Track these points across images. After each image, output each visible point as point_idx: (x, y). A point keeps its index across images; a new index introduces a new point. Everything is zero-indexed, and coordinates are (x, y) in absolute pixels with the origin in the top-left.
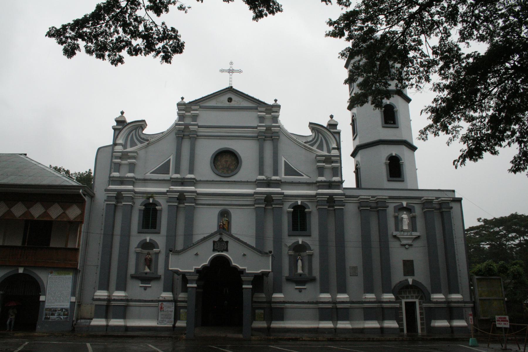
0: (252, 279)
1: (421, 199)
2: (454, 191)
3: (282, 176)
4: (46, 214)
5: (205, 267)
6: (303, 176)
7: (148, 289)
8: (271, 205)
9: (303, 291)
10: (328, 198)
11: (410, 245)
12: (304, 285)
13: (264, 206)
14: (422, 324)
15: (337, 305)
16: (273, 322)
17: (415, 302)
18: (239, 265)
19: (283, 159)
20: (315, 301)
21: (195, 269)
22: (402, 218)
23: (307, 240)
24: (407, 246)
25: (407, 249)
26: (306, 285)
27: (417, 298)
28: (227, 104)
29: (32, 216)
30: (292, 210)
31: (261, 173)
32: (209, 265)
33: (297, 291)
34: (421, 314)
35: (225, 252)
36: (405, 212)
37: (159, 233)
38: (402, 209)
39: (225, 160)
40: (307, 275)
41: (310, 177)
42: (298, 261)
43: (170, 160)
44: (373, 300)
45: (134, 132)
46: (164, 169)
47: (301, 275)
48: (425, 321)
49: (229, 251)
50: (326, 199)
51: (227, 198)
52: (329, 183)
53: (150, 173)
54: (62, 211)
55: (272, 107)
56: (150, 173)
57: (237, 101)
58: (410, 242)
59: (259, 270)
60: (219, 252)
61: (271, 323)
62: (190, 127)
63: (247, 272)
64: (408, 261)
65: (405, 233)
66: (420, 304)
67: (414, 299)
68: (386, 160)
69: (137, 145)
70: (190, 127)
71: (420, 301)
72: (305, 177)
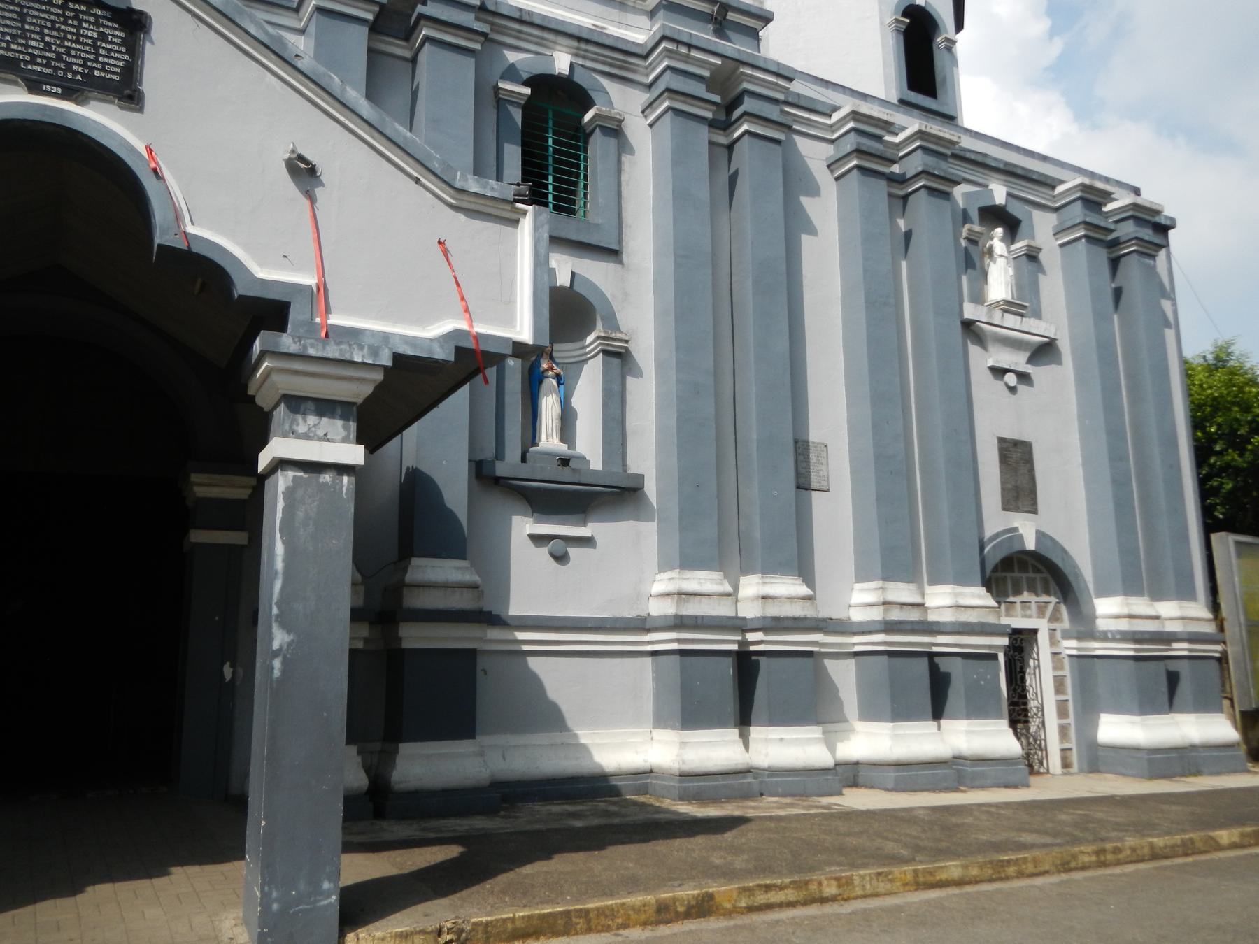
0: (368, 390)
1: (1053, 188)
8: (408, 34)
10: (715, 70)
11: (1023, 377)
12: (585, 525)
13: (370, 17)
14: (1063, 731)
15: (751, 637)
16: (406, 749)
17: (1035, 631)
18: (246, 247)
20: (628, 613)
22: (990, 251)
23: (595, 272)
24: (1011, 379)
25: (1013, 390)
26: (590, 525)
27: (1041, 609)
30: (527, 91)
33: (543, 552)
35: (113, 108)
36: (999, 231)
38: (995, 215)
40: (596, 464)
42: (541, 382)
44: (914, 616)
47: (565, 462)
48: (1071, 720)
49: (148, 103)
50: (706, 74)
58: (1018, 360)
59: (422, 322)
60: (34, 86)
61: (389, 757)
64: (1016, 443)
65: (1006, 315)
66: (1053, 642)
67: (1030, 617)
68: (896, 13)
71: (1054, 625)
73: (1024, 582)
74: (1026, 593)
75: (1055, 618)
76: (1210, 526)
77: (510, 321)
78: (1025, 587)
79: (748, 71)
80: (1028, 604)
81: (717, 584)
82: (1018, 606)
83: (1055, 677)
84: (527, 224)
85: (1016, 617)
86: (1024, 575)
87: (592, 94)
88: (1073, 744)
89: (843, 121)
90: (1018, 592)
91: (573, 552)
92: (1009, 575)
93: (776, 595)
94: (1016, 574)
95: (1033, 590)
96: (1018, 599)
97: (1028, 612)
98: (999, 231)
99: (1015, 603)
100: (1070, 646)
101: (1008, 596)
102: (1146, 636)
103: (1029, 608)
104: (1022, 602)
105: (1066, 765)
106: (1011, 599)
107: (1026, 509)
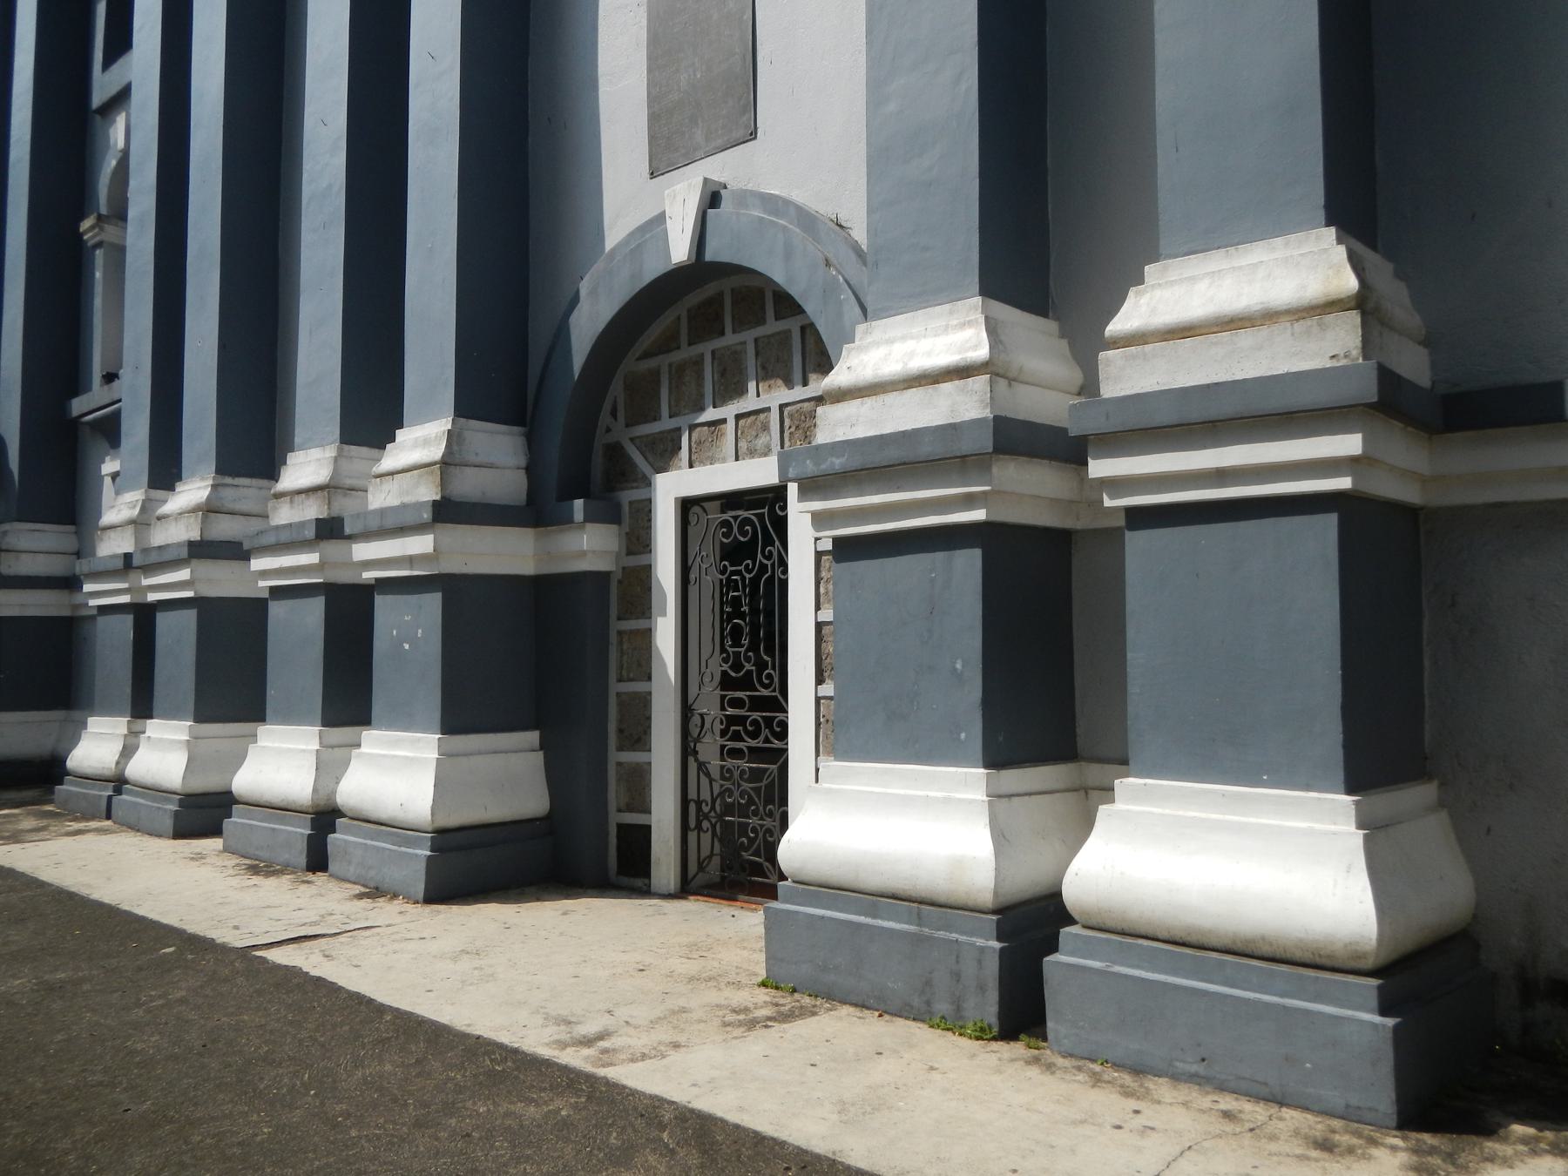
73: (751, 362)
74: (752, 386)
78: (751, 362)
80: (762, 416)
81: (130, 508)
82: (730, 426)
83: (819, 626)
85: (724, 460)
86: (748, 336)
90: (731, 388)
92: (706, 348)
93: (168, 513)
94: (730, 339)
95: (775, 368)
96: (729, 411)
97: (762, 441)
99: (724, 421)
101: (702, 409)
102: (838, 463)
103: (765, 427)
104: (738, 417)
106: (710, 414)
107: (719, 142)
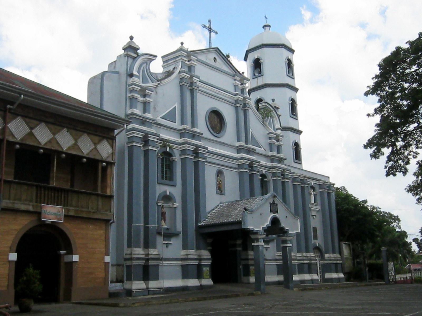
2: (329, 178)
3: (250, 146)
4: (75, 146)
5: (268, 227)
6: (261, 148)
7: (170, 246)
9: (268, 249)
10: (282, 171)
11: (315, 216)
12: (268, 245)
19: (251, 130)
21: (263, 228)
28: (212, 62)
29: (60, 146)
30: (261, 177)
31: (238, 140)
32: (270, 225)
34: (320, 269)
37: (175, 186)
39: (216, 120)
41: (265, 150)
43: (175, 107)
45: (145, 65)
46: (170, 116)
51: (221, 158)
52: (279, 158)
53: (161, 118)
54: (93, 146)
55: (244, 79)
56: (161, 118)
57: (220, 64)
60: (274, 213)
62: (194, 78)
63: (289, 232)
69: (149, 83)
70: (194, 78)
72: (262, 149)
75: (319, 258)
76: (340, 240)
77: (298, 230)
79: (286, 171)
84: (299, 220)
87: (267, 176)
88: (321, 279)
89: (295, 175)
91: (268, 249)
98: (312, 190)
100: (322, 262)
105: (321, 282)
